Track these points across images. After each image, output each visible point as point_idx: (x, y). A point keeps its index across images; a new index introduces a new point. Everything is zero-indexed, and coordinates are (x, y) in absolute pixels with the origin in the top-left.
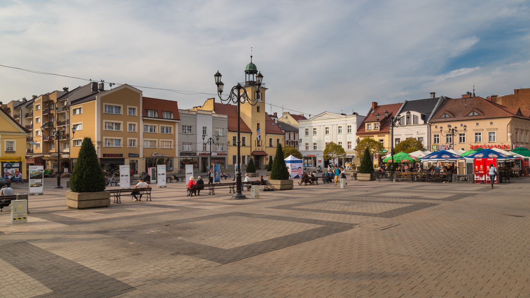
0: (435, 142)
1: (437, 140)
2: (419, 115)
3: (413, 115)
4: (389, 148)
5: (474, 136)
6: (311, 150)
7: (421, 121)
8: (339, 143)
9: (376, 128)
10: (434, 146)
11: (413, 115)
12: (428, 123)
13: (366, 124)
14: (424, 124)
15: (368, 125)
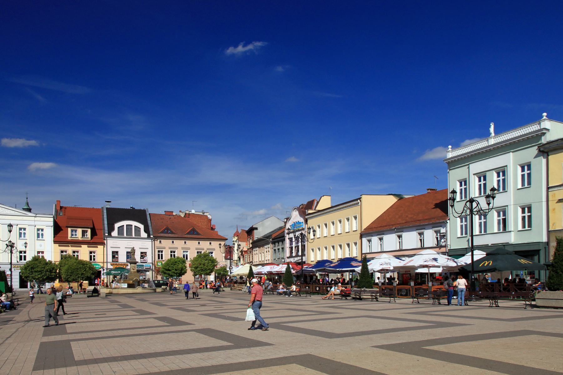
0: (159, 258)
1: (160, 257)
2: (142, 227)
3: (135, 226)
4: (104, 262)
5: (170, 253)
6: (8, 262)
7: (144, 234)
8: (39, 252)
9: (73, 236)
10: (159, 262)
11: (135, 226)
12: (152, 236)
13: (69, 229)
14: (147, 237)
15: (72, 231)
